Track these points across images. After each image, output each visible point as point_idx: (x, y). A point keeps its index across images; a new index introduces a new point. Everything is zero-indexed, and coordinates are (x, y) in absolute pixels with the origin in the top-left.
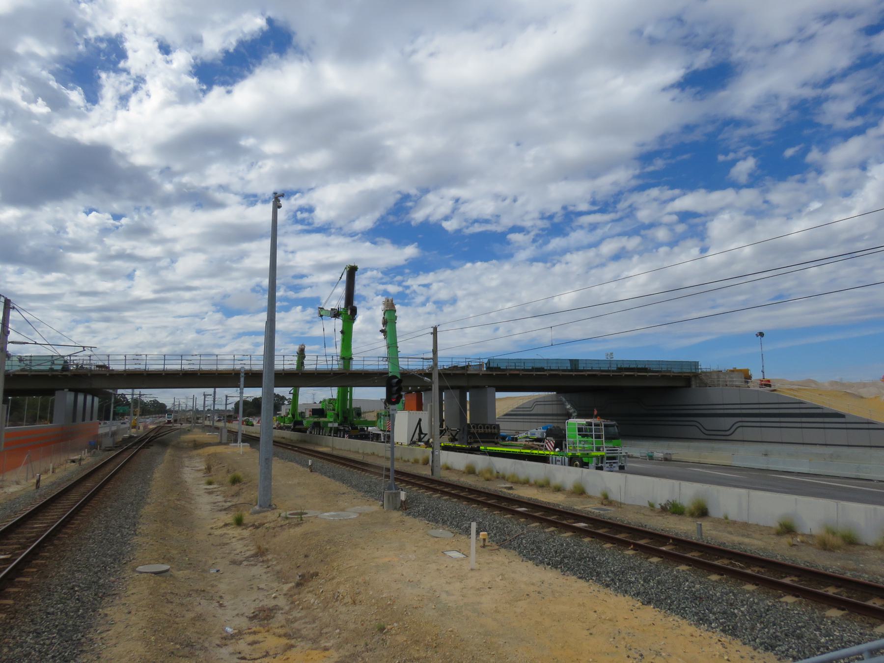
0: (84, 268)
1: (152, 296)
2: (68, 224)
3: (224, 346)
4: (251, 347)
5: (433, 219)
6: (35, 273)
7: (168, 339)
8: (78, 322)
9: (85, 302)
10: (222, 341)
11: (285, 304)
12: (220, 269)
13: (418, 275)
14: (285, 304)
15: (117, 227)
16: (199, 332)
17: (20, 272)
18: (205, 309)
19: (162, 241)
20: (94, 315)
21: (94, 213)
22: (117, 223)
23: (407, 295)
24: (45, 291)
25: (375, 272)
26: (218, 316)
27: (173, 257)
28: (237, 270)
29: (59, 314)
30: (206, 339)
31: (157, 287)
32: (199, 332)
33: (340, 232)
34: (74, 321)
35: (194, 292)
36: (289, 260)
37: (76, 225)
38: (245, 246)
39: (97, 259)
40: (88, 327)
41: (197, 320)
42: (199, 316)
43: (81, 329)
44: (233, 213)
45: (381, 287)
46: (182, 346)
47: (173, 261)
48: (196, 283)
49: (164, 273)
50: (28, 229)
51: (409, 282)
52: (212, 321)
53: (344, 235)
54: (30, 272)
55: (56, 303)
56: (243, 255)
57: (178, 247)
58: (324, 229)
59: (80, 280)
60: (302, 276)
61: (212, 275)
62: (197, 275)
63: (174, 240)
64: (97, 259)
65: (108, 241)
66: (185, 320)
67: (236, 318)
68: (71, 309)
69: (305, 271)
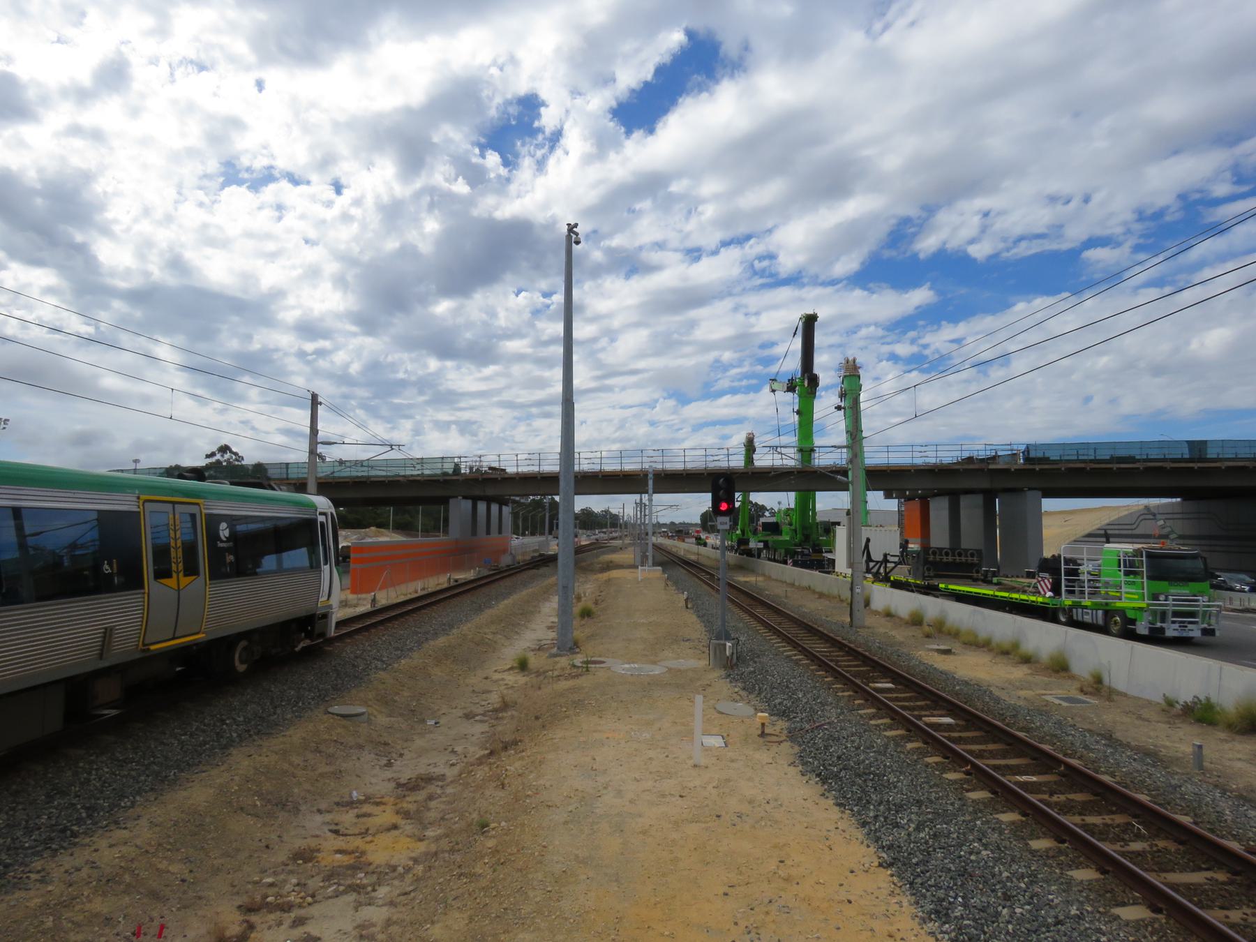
0: (520, 358)
1: (593, 385)
2: (499, 309)
3: (683, 440)
4: (716, 441)
5: (953, 245)
6: (472, 367)
7: (617, 434)
8: (519, 419)
9: (525, 396)
10: (680, 434)
11: (754, 382)
12: (665, 344)
13: (939, 327)
14: (754, 382)
15: (548, 306)
16: (652, 423)
17: (459, 368)
18: (656, 396)
19: (596, 318)
20: (534, 410)
21: (523, 294)
22: (547, 301)
23: (926, 357)
24: (482, 387)
25: (872, 328)
26: (671, 403)
27: (612, 335)
28: (688, 343)
29: (500, 411)
30: (661, 433)
31: (599, 373)
32: (652, 423)
33: (816, 282)
34: (515, 418)
35: (640, 376)
36: (753, 326)
37: (507, 310)
38: (693, 314)
39: (532, 346)
40: (529, 425)
41: (646, 410)
42: (652, 405)
43: (522, 428)
44: (672, 274)
45: (886, 349)
46: (634, 443)
47: (613, 340)
48: (641, 364)
49: (602, 356)
50: (460, 320)
51: (928, 339)
52: (664, 410)
53: (825, 284)
54: (468, 367)
55: (495, 399)
56: (693, 324)
57: (616, 323)
58: (794, 280)
59: (517, 370)
60: (773, 344)
61: (658, 353)
62: (642, 355)
63: (609, 315)
64: (532, 346)
65: (540, 325)
66: (634, 410)
67: (693, 404)
68: (510, 405)
69: (775, 338)
